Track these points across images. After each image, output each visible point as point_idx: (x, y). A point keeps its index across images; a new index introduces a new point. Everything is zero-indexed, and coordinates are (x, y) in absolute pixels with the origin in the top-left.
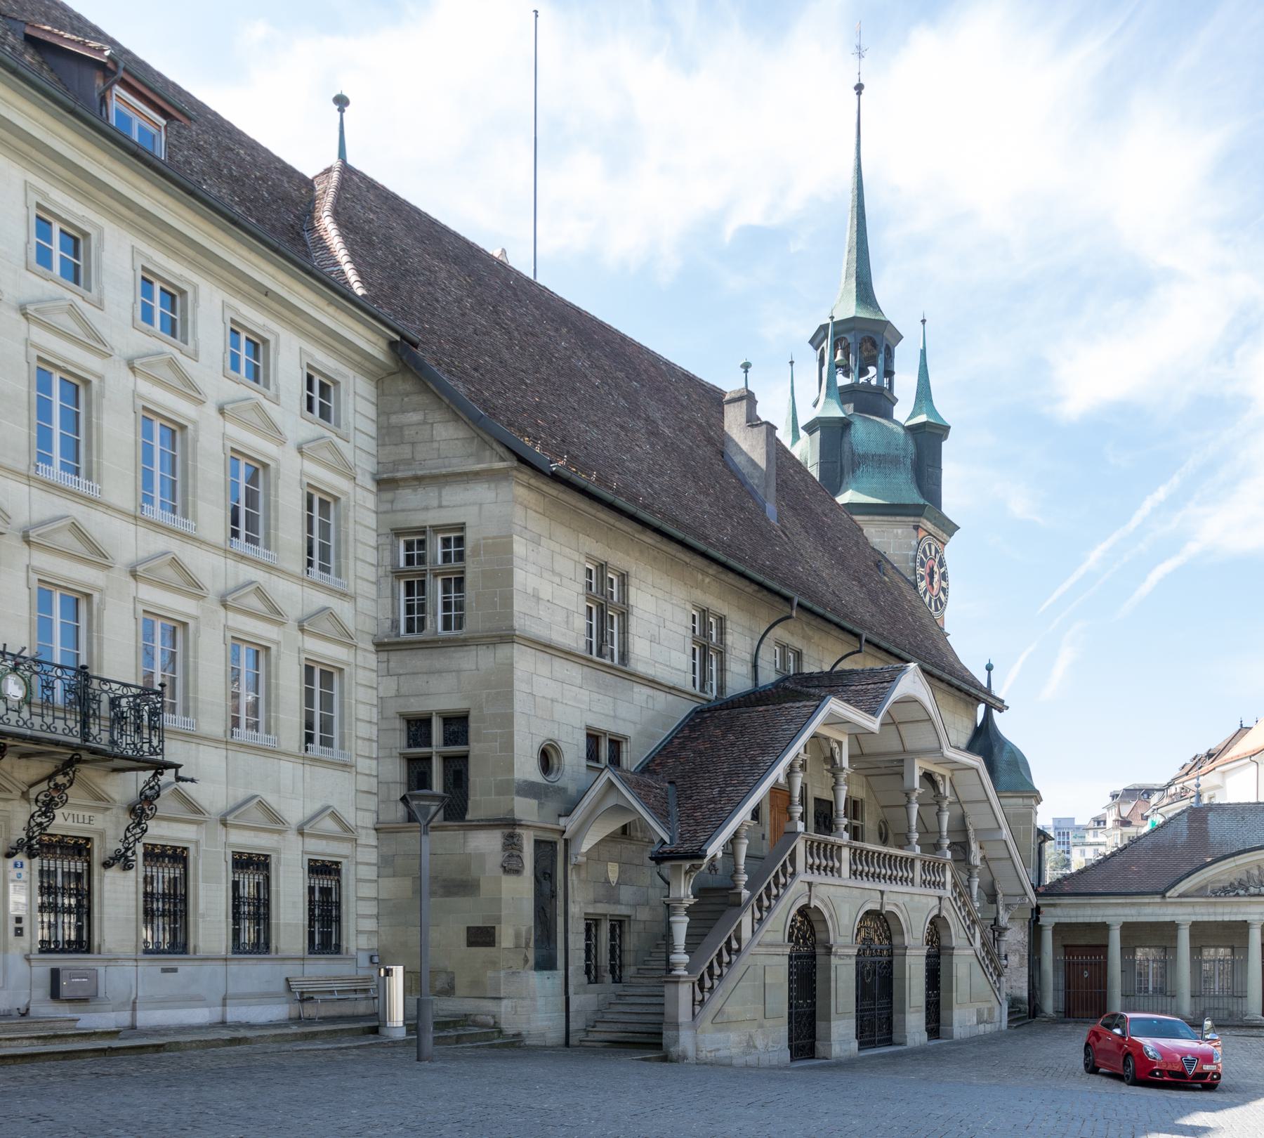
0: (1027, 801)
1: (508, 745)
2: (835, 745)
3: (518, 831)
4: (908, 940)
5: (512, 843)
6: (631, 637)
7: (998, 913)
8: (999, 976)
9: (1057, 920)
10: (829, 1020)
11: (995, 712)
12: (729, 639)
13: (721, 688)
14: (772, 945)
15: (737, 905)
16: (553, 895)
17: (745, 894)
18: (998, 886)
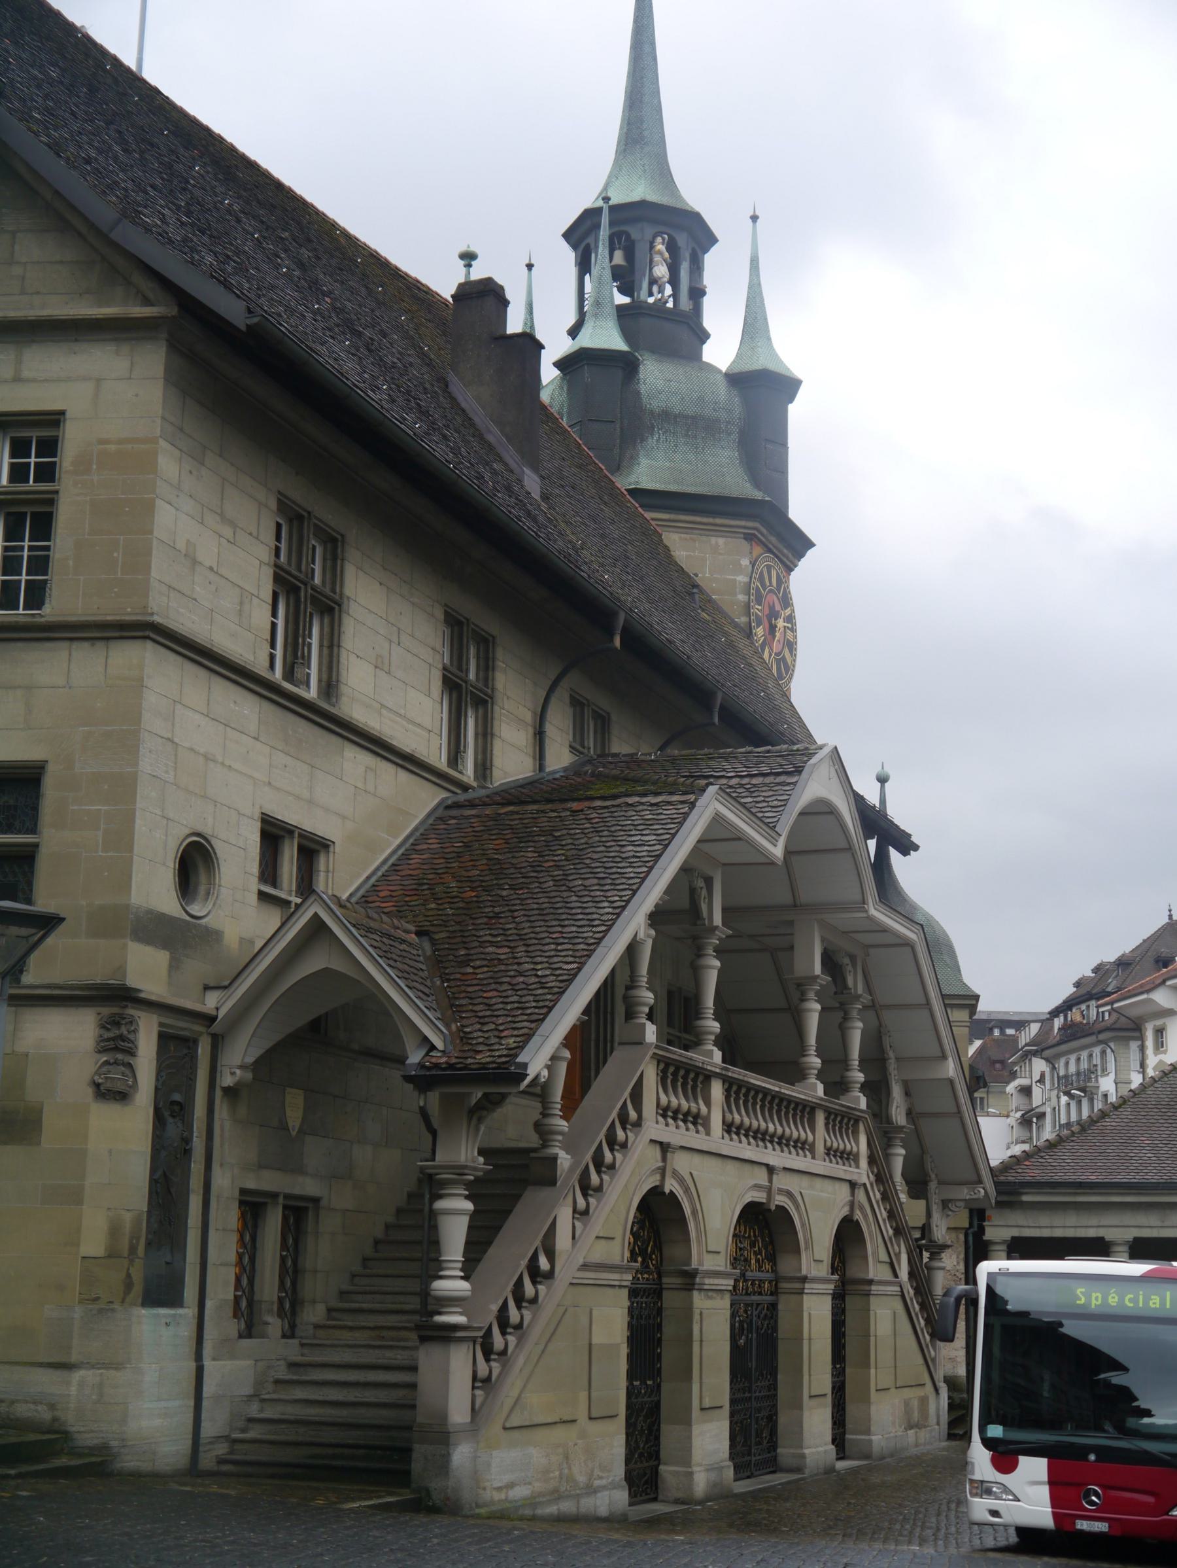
1: (122, 837)
2: (701, 883)
5: (116, 1044)
6: (343, 654)
7: (929, 1215)
9: (1016, 1232)
10: (688, 1423)
11: (894, 854)
13: (484, 768)
15: (547, 1175)
17: (564, 1160)
18: (929, 1166)
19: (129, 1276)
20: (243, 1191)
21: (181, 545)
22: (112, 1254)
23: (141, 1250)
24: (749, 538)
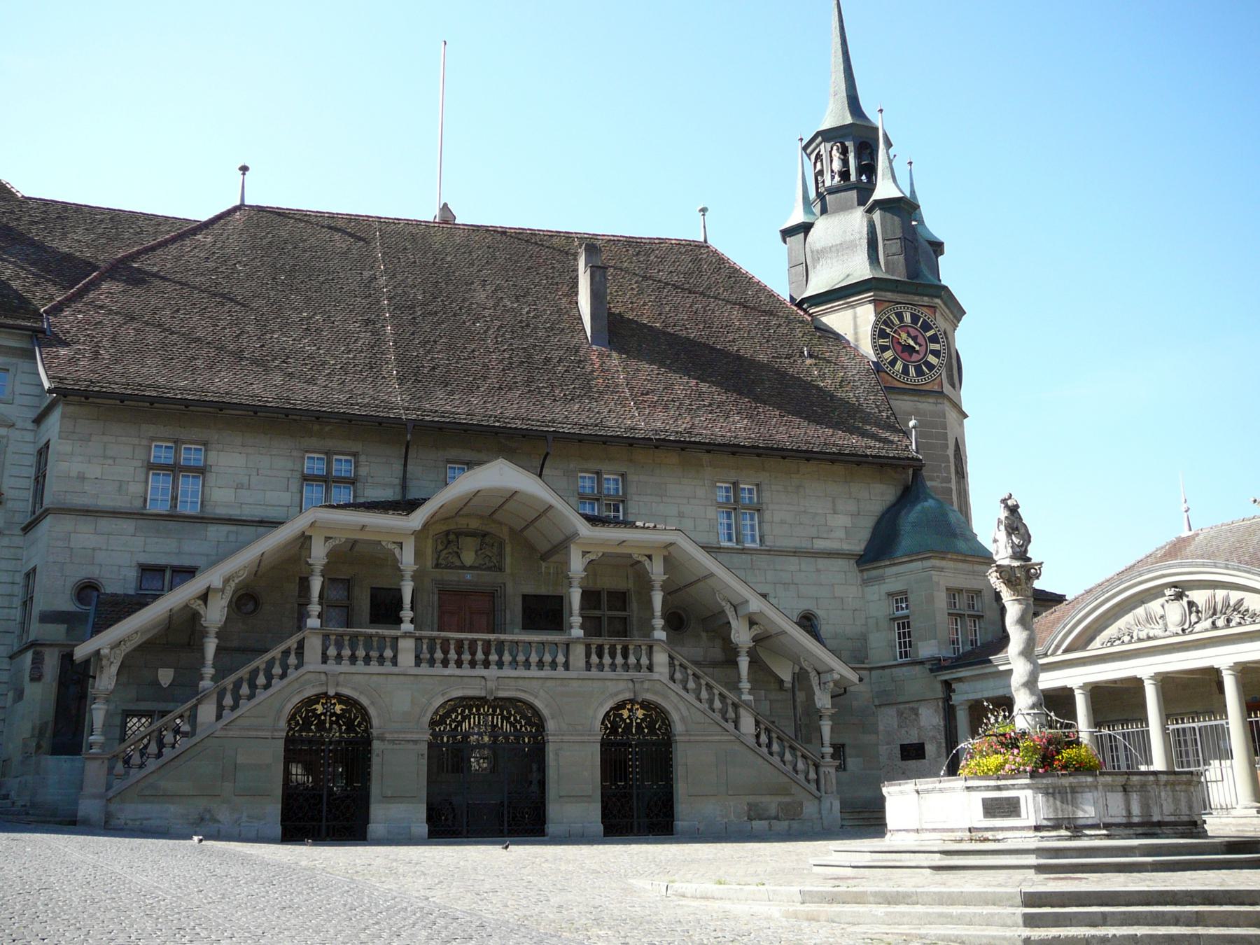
3: (38, 649)
4: (551, 725)
5: (38, 661)
8: (817, 766)
9: (965, 697)
12: (363, 471)
17: (206, 684)
21: (74, 474)
22: (33, 736)
23: (49, 733)
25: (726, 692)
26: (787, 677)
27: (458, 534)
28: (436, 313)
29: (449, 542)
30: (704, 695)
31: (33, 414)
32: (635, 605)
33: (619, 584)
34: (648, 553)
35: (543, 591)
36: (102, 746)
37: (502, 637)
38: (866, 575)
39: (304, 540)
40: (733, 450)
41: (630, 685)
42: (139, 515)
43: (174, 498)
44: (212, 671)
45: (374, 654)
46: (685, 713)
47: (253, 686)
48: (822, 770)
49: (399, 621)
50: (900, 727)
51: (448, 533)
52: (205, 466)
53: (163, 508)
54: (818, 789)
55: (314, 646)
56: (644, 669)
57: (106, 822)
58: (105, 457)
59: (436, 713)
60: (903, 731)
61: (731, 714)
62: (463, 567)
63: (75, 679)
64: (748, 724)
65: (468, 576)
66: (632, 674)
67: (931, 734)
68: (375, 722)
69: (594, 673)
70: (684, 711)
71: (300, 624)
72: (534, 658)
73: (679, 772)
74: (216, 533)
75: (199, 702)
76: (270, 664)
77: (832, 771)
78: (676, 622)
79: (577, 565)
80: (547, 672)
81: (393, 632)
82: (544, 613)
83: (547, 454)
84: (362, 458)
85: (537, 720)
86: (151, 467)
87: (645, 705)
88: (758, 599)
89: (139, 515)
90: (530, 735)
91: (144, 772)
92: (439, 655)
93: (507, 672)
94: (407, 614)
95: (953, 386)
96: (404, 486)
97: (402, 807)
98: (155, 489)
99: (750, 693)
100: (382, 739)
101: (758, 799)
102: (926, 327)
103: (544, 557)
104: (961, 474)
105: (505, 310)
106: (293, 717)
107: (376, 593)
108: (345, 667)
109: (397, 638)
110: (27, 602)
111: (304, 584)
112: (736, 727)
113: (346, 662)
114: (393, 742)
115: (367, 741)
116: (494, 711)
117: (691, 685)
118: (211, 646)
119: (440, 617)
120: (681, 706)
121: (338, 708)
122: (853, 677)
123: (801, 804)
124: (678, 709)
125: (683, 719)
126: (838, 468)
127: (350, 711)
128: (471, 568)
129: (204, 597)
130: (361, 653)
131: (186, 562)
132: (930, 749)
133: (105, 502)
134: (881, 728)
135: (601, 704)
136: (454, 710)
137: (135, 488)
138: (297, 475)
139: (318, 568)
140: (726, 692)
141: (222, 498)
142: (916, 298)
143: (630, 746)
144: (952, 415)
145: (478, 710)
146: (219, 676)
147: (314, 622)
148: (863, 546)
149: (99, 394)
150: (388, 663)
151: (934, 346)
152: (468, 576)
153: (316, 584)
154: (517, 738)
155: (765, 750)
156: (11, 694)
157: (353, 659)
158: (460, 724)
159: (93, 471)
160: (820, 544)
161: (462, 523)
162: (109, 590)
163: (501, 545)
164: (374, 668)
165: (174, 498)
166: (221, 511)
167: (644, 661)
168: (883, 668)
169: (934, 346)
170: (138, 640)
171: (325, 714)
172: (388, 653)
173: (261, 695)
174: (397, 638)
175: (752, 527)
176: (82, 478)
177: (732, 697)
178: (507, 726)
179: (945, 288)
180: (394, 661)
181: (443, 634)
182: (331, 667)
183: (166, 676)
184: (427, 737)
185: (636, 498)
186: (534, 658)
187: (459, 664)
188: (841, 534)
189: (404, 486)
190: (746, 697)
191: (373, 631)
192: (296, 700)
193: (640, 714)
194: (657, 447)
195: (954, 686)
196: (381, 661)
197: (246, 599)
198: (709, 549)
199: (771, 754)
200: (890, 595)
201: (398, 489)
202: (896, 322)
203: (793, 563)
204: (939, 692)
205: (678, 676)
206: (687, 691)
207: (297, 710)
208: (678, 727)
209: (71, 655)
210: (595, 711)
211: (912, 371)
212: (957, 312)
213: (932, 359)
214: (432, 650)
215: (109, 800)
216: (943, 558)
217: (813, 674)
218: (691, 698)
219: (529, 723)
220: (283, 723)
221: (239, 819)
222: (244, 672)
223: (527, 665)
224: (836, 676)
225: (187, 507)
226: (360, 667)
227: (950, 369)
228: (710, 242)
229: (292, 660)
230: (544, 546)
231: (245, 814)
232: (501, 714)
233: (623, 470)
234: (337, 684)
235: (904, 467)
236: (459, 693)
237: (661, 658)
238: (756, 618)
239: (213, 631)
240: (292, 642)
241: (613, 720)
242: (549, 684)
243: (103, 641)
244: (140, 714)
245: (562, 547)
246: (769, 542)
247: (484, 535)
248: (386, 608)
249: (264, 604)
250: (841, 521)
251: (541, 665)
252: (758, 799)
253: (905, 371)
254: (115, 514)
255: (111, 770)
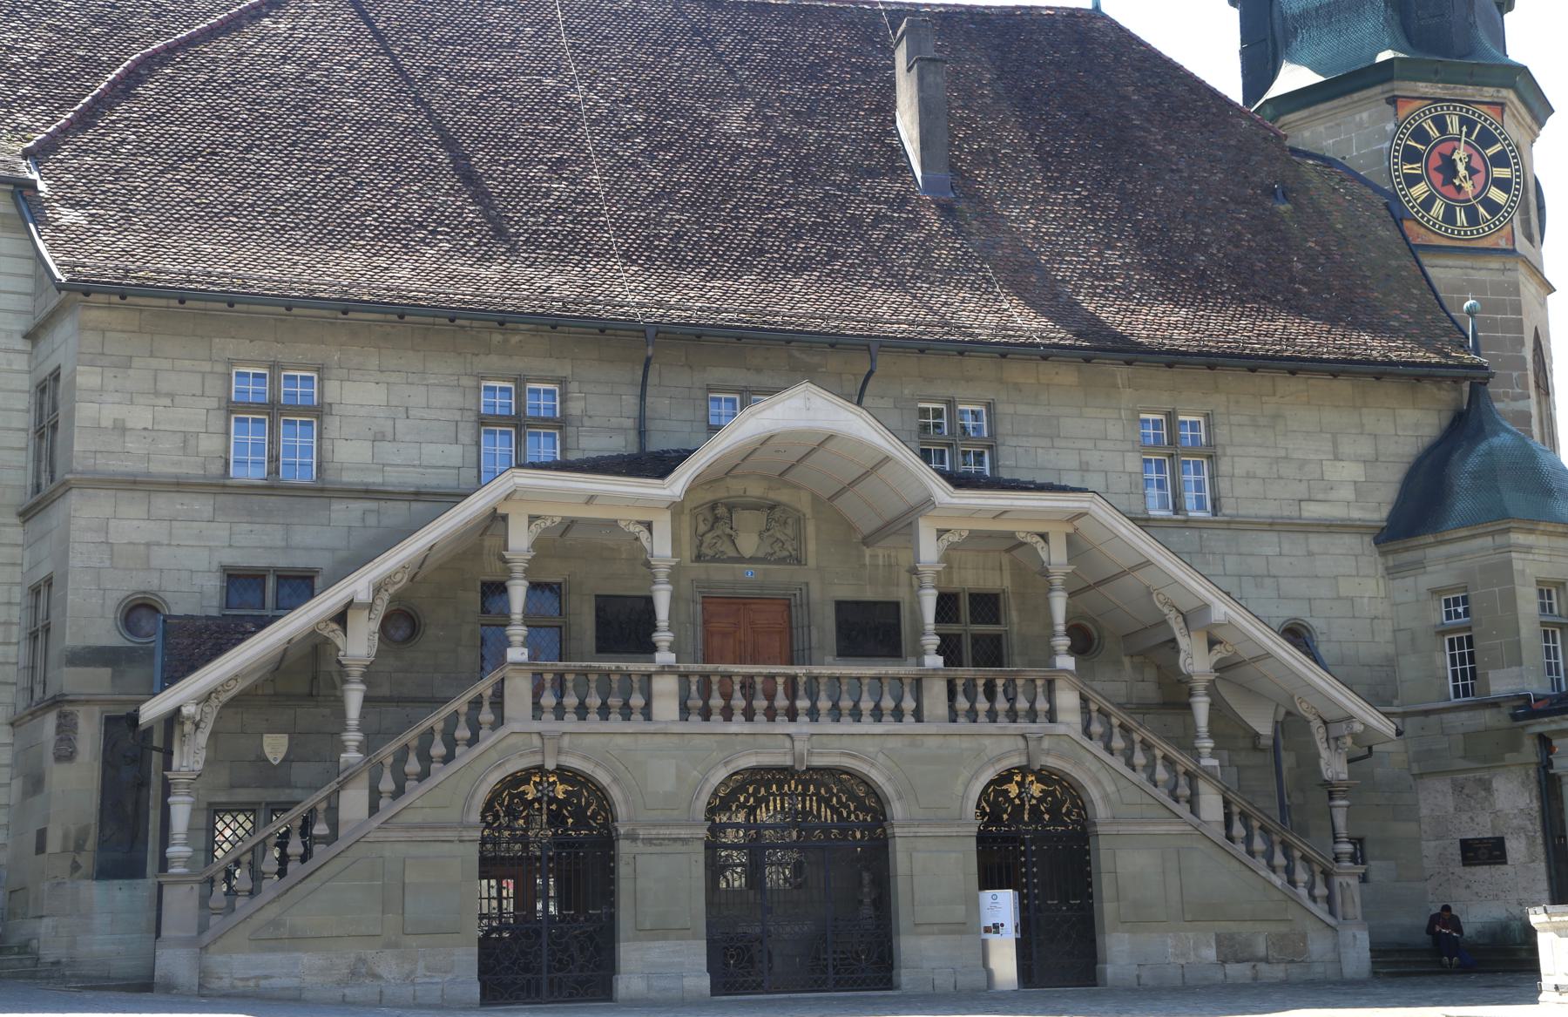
0: (1500, 540)
3: (67, 708)
4: (897, 810)
8: (1327, 876)
12: (575, 408)
14: (421, 827)
16: (143, 783)
17: (351, 756)
19: (75, 862)
20: (210, 804)
21: (107, 422)
22: (64, 851)
23: (91, 843)
24: (1393, 101)
25: (1174, 754)
26: (1264, 728)
27: (731, 508)
28: (670, 144)
29: (717, 519)
30: (1139, 759)
31: (22, 325)
32: (1014, 616)
33: (990, 581)
34: (1041, 529)
35: (869, 594)
36: (189, 862)
37: (816, 670)
38: (1391, 561)
39: (495, 520)
40: (1172, 359)
41: (1021, 743)
42: (219, 487)
43: (274, 459)
44: (358, 736)
45: (615, 702)
46: (1110, 788)
47: (425, 758)
48: (1337, 880)
49: (652, 648)
50: (1458, 809)
51: (714, 506)
52: (321, 405)
53: (254, 474)
54: (1332, 912)
55: (519, 691)
56: (1042, 718)
57: (200, 985)
58: (157, 394)
59: (715, 794)
60: (1465, 817)
61: (1184, 791)
62: (741, 559)
63: (133, 756)
64: (1211, 805)
65: (749, 572)
66: (1023, 726)
67: (1515, 822)
68: (621, 810)
69: (963, 725)
70: (1105, 783)
71: (501, 660)
72: (867, 705)
73: (1106, 887)
74: (346, 513)
75: (342, 786)
76: (452, 721)
77: (1354, 882)
78: (1083, 641)
79: (929, 550)
80: (888, 726)
81: (643, 667)
82: (871, 629)
83: (871, 373)
84: (573, 387)
85: (874, 806)
86: (231, 408)
87: (1044, 776)
88: (1221, 605)
89: (219, 487)
90: (863, 826)
91: (259, 901)
92: (716, 702)
93: (826, 726)
94: (663, 637)
95: (1530, 239)
96: (642, 433)
97: (669, 945)
98: (241, 446)
99: (1213, 756)
100: (632, 837)
101: (1233, 927)
102: (1487, 139)
103: (867, 541)
104: (1544, 388)
105: (782, 139)
106: (489, 806)
107: (604, 604)
108: (570, 723)
109: (648, 676)
110: (39, 634)
111: (495, 590)
112: (1194, 811)
113: (571, 717)
114: (649, 841)
115: (606, 843)
116: (806, 789)
117: (1118, 743)
118: (354, 698)
119: (706, 643)
120: (1104, 777)
121: (560, 791)
122: (1387, 727)
123: (1304, 937)
124: (1098, 782)
125: (1106, 797)
126: (1343, 386)
127: (579, 795)
128: (753, 560)
129: (341, 618)
130: (594, 701)
131: (300, 561)
132: (1516, 848)
133: (162, 467)
134: (1424, 812)
135: (975, 776)
136: (742, 788)
137: (210, 444)
138: (471, 416)
139: (519, 567)
140: (1174, 754)
141: (351, 456)
142: (1470, 90)
143: (1023, 842)
144: (1529, 289)
145: (780, 788)
146: (367, 747)
147: (517, 654)
148: (1384, 513)
149: (144, 290)
150: (637, 717)
151: (1501, 173)
152: (749, 572)
153: (518, 594)
154: (843, 831)
155: (1242, 848)
156: (17, 785)
157: (582, 711)
158: (752, 811)
159: (139, 416)
160: (1312, 511)
161: (735, 488)
162: (177, 610)
163: (800, 521)
164: (615, 723)
165: (274, 459)
166: (350, 478)
167: (1042, 705)
168: (1426, 713)
169: (1501, 173)
170: (236, 689)
171: (539, 800)
172: (637, 701)
173: (440, 773)
174: (648, 676)
175: (1199, 486)
176: (121, 429)
177: (1184, 762)
178: (826, 813)
179: (1523, 71)
180: (647, 713)
181: (722, 667)
182: (548, 724)
183: (275, 747)
184: (702, 832)
185: (1012, 441)
186: (867, 705)
187: (749, 715)
188: (1347, 493)
189: (642, 433)
190: (1207, 762)
191: (613, 665)
192: (495, 778)
193: (1036, 789)
194: (1045, 358)
195: (1555, 743)
196: (626, 712)
197: (403, 620)
198: (1143, 522)
199: (1251, 853)
200: (1435, 592)
201: (633, 436)
202: (1434, 133)
203: (1268, 544)
204: (1530, 751)
205: (1096, 728)
206: (1111, 752)
207: (495, 796)
208: (1101, 811)
209: (133, 719)
210: (967, 786)
211: (1461, 217)
212: (1539, 109)
213: (1496, 195)
214: (706, 693)
215: (205, 948)
216: (1531, 531)
217: (1316, 724)
218: (1118, 763)
219: (862, 807)
220: (475, 817)
221: (412, 972)
222: (410, 737)
223: (856, 715)
224: (1358, 728)
225: (300, 474)
226: (594, 723)
227: (1525, 211)
228: (1105, 9)
229: (486, 716)
230: (867, 525)
231: (421, 964)
232: (817, 794)
233: (990, 396)
234: (559, 752)
235: (1456, 380)
236: (751, 761)
237: (1067, 699)
238: (1219, 634)
239: (356, 672)
240: (485, 687)
241: (993, 802)
242: (892, 743)
243: (184, 693)
244: (233, 809)
245: (902, 526)
246: (1228, 509)
247: (772, 507)
248: (626, 626)
249: (446, 623)
250: (1350, 471)
251: (877, 714)
252: (1233, 927)
253: (1449, 217)
254: (179, 485)
255: (204, 902)
